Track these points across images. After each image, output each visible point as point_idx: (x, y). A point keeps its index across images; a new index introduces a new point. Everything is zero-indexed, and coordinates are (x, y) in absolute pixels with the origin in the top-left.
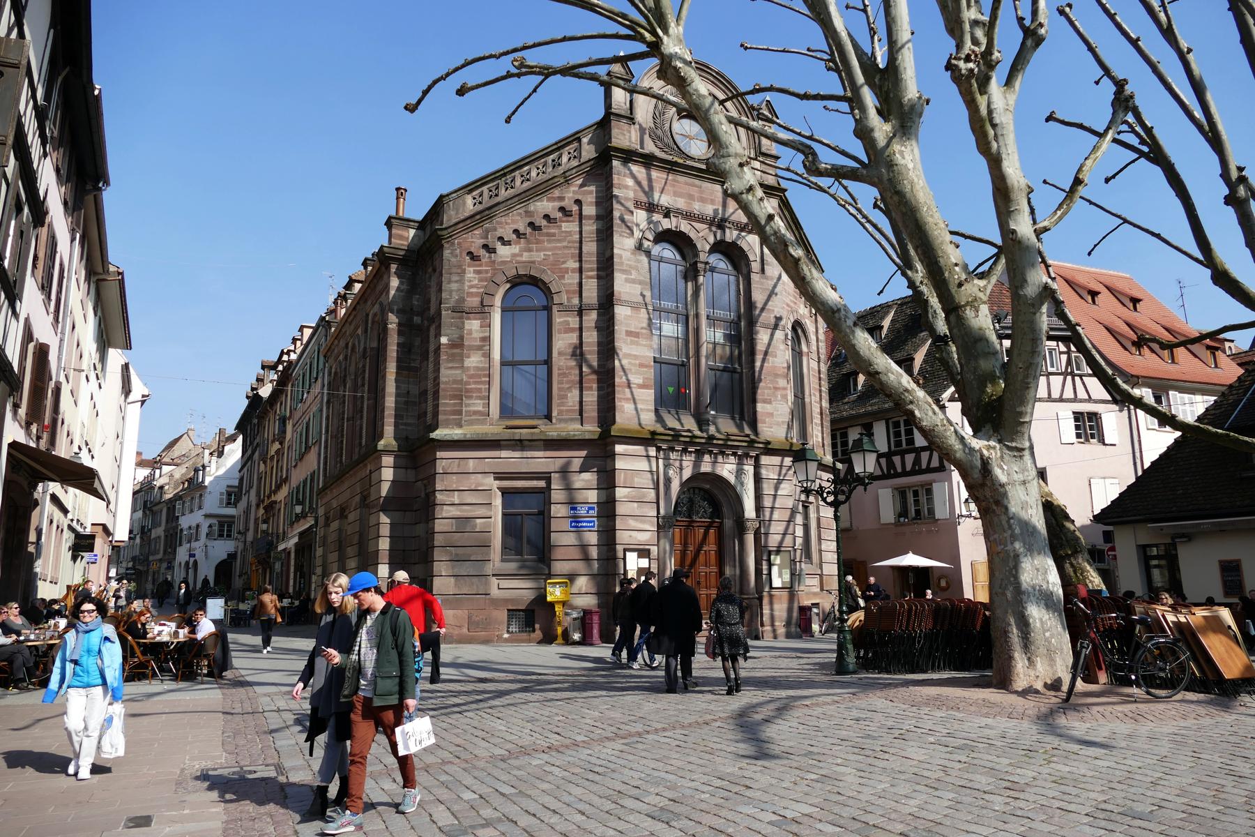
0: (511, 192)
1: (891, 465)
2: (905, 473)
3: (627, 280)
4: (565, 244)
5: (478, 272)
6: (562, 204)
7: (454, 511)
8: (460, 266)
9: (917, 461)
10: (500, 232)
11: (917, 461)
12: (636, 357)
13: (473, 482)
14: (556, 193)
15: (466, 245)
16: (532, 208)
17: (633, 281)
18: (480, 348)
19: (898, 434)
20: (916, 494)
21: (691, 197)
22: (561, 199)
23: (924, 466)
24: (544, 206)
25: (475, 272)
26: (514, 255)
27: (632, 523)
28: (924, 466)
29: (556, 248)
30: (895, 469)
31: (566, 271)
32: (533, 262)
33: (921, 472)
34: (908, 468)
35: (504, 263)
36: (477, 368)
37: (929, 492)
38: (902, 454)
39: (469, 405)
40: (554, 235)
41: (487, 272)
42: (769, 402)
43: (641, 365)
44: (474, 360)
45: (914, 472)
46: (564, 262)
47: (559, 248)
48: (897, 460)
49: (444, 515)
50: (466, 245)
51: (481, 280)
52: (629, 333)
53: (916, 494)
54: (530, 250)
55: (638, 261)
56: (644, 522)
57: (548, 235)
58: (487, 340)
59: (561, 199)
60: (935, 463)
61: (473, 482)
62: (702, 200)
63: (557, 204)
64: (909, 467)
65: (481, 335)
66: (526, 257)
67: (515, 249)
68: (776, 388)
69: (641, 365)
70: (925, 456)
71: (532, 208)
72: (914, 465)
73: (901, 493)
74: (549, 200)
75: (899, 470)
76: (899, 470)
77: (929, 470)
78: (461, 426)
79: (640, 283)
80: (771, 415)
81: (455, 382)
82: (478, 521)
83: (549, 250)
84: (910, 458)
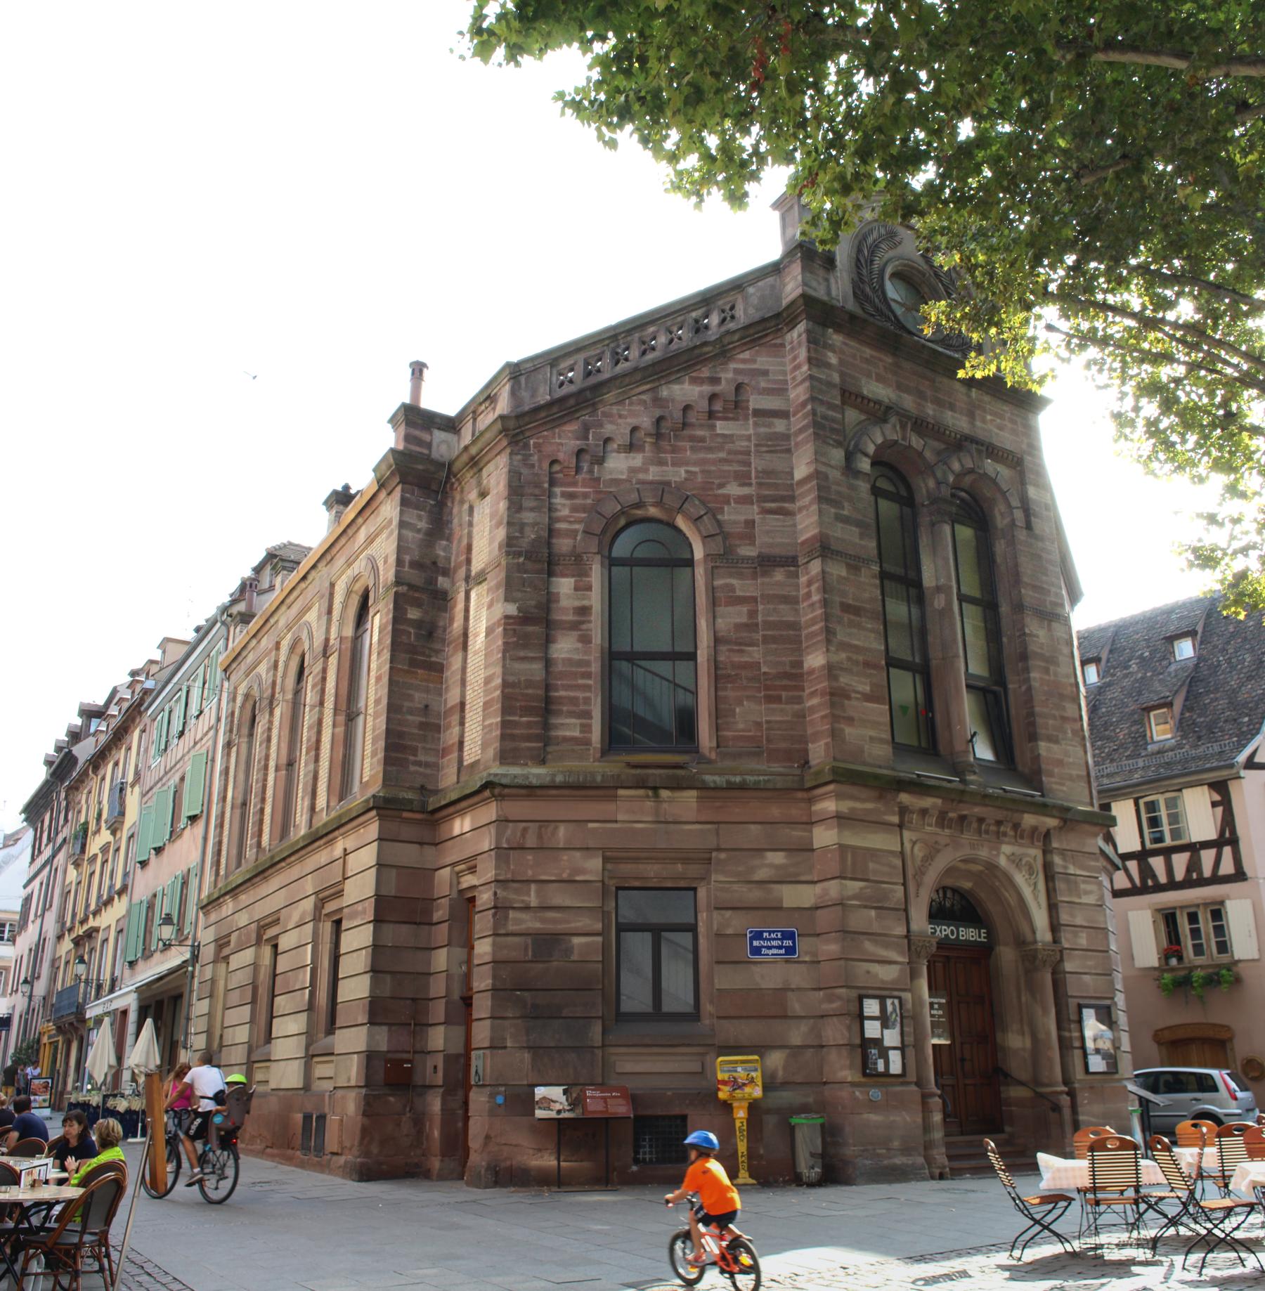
0: (623, 366)
1: (1147, 872)
2: (1173, 885)
3: (839, 518)
4: (722, 455)
5: (571, 496)
6: (717, 389)
7: (530, 923)
8: (538, 485)
9: (1194, 865)
10: (608, 429)
11: (1194, 865)
12: (857, 649)
13: (567, 863)
14: (705, 372)
15: (548, 449)
16: (664, 392)
17: (846, 520)
18: (575, 626)
19: (1154, 822)
20: (1193, 918)
21: (921, 395)
22: (715, 380)
23: (1207, 873)
24: (684, 391)
25: (564, 495)
26: (632, 470)
27: (869, 946)
28: (1207, 873)
29: (703, 462)
30: (1154, 877)
31: (726, 499)
32: (668, 483)
33: (1202, 882)
34: (1179, 875)
35: (616, 482)
36: (569, 661)
37: (1217, 914)
38: (1167, 852)
39: (556, 727)
40: (702, 440)
41: (585, 496)
42: (1055, 741)
43: (867, 664)
44: (564, 647)
45: (1188, 883)
46: (721, 486)
47: (714, 462)
48: (1157, 863)
49: (511, 928)
50: (548, 449)
51: (574, 509)
52: (846, 608)
53: (1193, 918)
54: (661, 463)
55: (853, 488)
56: (887, 946)
57: (692, 438)
58: (584, 611)
59: (715, 380)
60: (1227, 867)
61: (567, 863)
62: (938, 403)
63: (707, 389)
64: (1179, 875)
65: (577, 604)
66: (653, 473)
67: (637, 460)
68: (1064, 719)
69: (867, 664)
70: (1208, 857)
71: (664, 392)
72: (1189, 871)
73: (1169, 918)
74: (695, 381)
75: (1163, 879)
76: (1163, 879)
77: (1216, 879)
78: (543, 762)
79: (858, 524)
80: (1060, 763)
81: (529, 684)
82: (576, 941)
83: (695, 464)
84: (1180, 862)
